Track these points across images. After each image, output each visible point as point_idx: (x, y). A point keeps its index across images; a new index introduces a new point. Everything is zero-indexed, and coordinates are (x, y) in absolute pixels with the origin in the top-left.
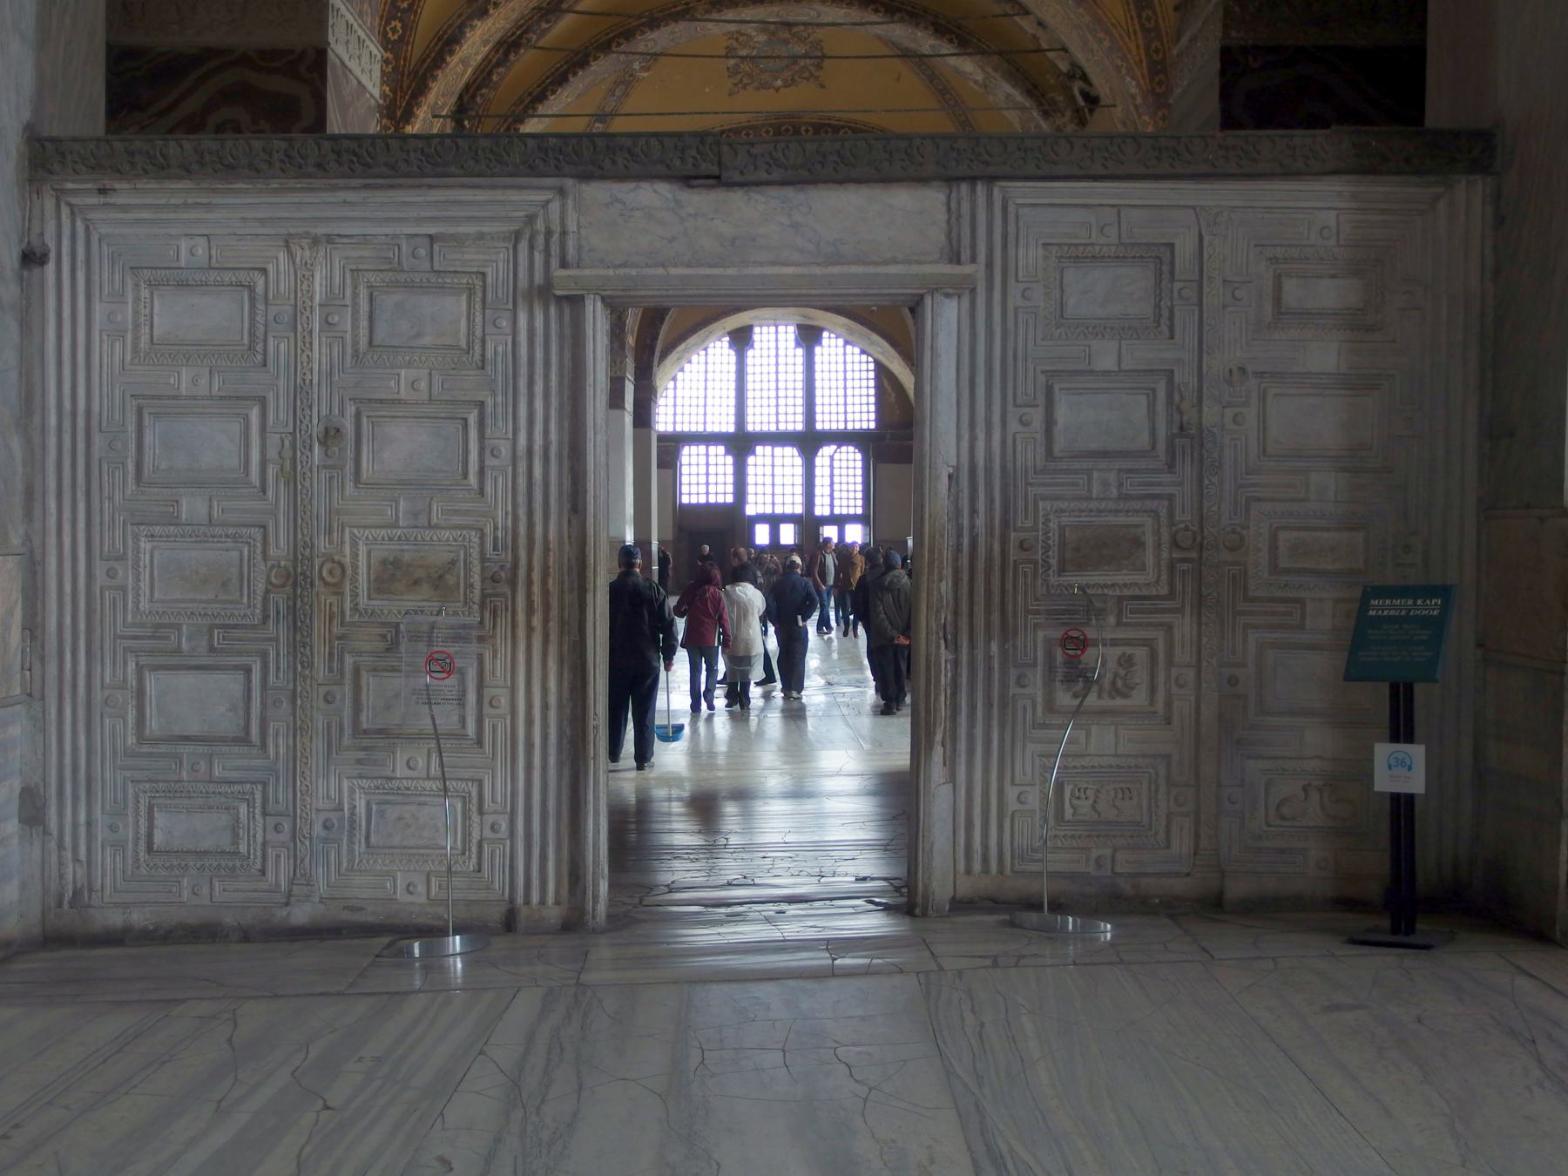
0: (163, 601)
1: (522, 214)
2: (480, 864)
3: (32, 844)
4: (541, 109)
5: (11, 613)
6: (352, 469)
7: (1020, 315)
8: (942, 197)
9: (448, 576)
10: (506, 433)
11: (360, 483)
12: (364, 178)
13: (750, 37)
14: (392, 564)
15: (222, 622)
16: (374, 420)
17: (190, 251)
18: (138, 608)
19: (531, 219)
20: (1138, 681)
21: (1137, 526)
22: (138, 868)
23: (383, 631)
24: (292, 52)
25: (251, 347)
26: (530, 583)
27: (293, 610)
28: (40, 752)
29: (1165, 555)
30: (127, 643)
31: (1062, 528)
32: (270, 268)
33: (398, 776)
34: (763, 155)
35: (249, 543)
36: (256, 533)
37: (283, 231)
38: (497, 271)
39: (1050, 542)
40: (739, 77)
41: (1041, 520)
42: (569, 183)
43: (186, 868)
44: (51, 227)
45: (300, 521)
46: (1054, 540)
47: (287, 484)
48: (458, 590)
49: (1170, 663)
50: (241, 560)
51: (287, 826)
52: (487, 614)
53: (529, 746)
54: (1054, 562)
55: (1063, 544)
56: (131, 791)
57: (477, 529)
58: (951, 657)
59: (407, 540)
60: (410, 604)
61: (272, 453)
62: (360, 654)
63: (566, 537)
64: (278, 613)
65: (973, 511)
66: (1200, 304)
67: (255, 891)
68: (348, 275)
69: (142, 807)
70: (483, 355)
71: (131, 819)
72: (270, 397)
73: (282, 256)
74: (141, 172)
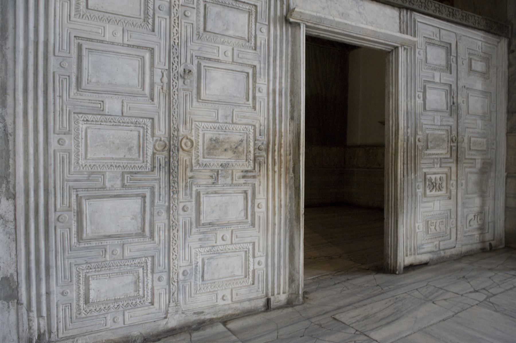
0: (93, 159)
3: (9, 312)
11: (200, 99)
14: (215, 140)
15: (128, 170)
16: (206, 68)
18: (78, 163)
22: (80, 314)
23: (211, 174)
25: (146, 20)
26: (274, 151)
28: (13, 253)
33: (218, 245)
36: (149, 122)
45: (172, 117)
48: (244, 153)
50: (139, 136)
51: (165, 277)
52: (257, 165)
56: (74, 270)
60: (222, 160)
61: (157, 79)
62: (199, 186)
64: (160, 165)
67: (149, 314)
69: (81, 279)
71: (75, 287)
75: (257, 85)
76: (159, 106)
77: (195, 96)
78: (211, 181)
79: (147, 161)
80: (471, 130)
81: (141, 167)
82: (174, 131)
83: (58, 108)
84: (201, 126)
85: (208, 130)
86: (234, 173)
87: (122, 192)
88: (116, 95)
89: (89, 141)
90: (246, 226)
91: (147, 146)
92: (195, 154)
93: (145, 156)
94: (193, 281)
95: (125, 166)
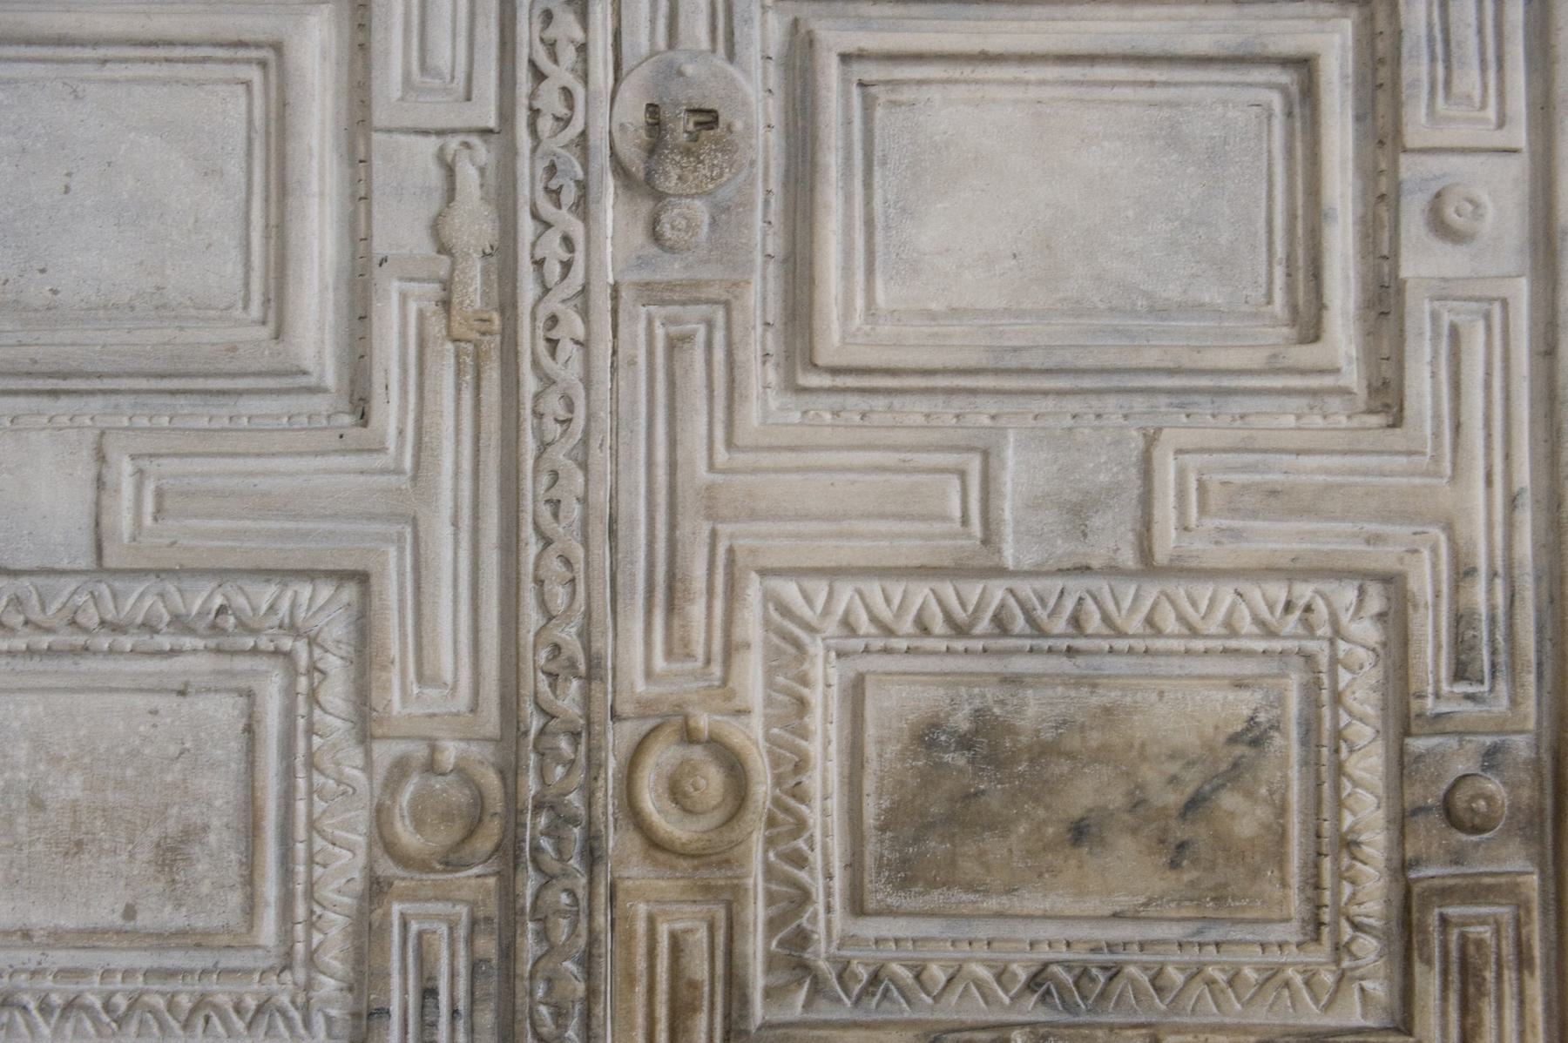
6: (774, 312)
9: (1229, 800)
10: (1501, 122)
14: (965, 743)
16: (872, 72)
35: (288, 656)
45: (532, 549)
48: (1281, 861)
50: (250, 730)
52: (1428, 982)
57: (1362, 576)
59: (1039, 631)
60: (1051, 930)
64: (428, 993)
75: (1409, 167)
76: (417, 464)
79: (311, 958)
81: (260, 1010)
82: (553, 676)
84: (827, 611)
85: (903, 644)
88: (54, 393)
91: (312, 825)
92: (769, 872)
93: (301, 911)
95: (121, 1002)
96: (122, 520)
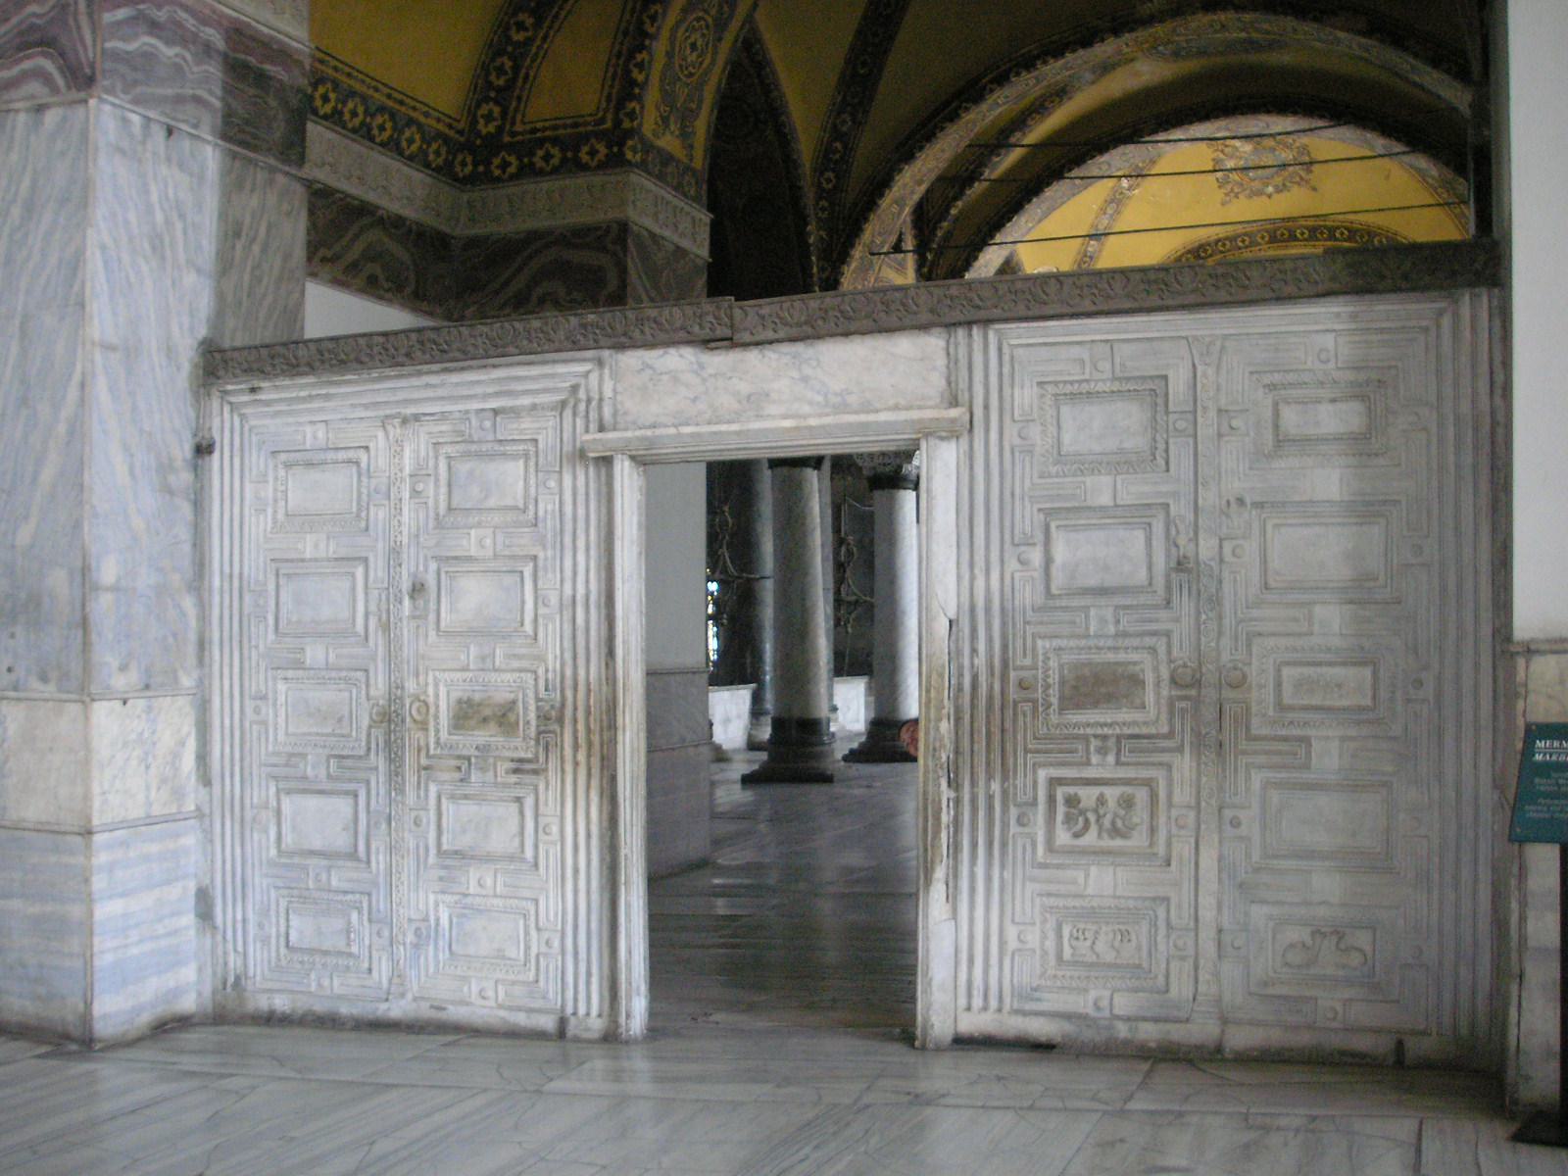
1: (568, 384)
2: (537, 975)
4: (998, 238)
5: (182, 743)
7: (1017, 454)
8: (942, 343)
12: (441, 362)
13: (1236, 149)
17: (314, 435)
19: (575, 388)
20: (1136, 820)
21: (1135, 663)
24: (601, 227)
25: (358, 516)
27: (388, 743)
28: (209, 858)
29: (1165, 692)
30: (269, 769)
31: (1061, 666)
32: (372, 445)
34: (770, 315)
37: (381, 413)
38: (547, 439)
39: (1050, 681)
40: (1229, 187)
41: (1041, 658)
42: (606, 353)
43: (314, 963)
44: (216, 422)
46: (1054, 678)
47: (384, 632)
49: (1170, 805)
51: (386, 933)
53: (576, 871)
54: (1054, 700)
55: (1062, 682)
58: (952, 795)
62: (443, 782)
63: (604, 678)
64: (378, 745)
65: (974, 651)
66: (1195, 436)
68: (431, 446)
70: (536, 513)
71: (274, 920)
72: (371, 559)
73: (381, 434)
74: (279, 371)
77: (432, 626)
78: (457, 775)
80: (1283, 642)
83: (254, 664)
86: (499, 764)
87: (329, 786)
89: (290, 709)
90: (524, 867)
94: (431, 948)
96: (331, 660)
